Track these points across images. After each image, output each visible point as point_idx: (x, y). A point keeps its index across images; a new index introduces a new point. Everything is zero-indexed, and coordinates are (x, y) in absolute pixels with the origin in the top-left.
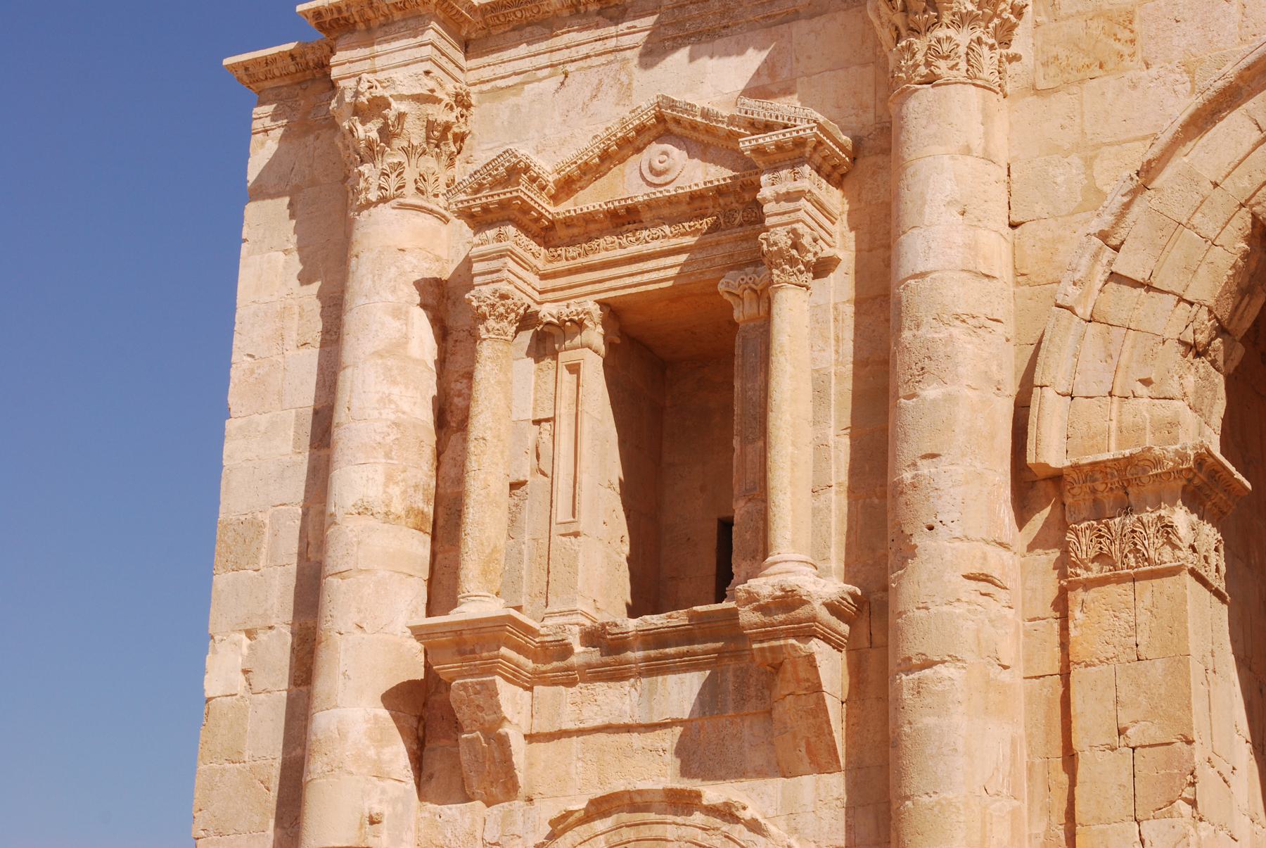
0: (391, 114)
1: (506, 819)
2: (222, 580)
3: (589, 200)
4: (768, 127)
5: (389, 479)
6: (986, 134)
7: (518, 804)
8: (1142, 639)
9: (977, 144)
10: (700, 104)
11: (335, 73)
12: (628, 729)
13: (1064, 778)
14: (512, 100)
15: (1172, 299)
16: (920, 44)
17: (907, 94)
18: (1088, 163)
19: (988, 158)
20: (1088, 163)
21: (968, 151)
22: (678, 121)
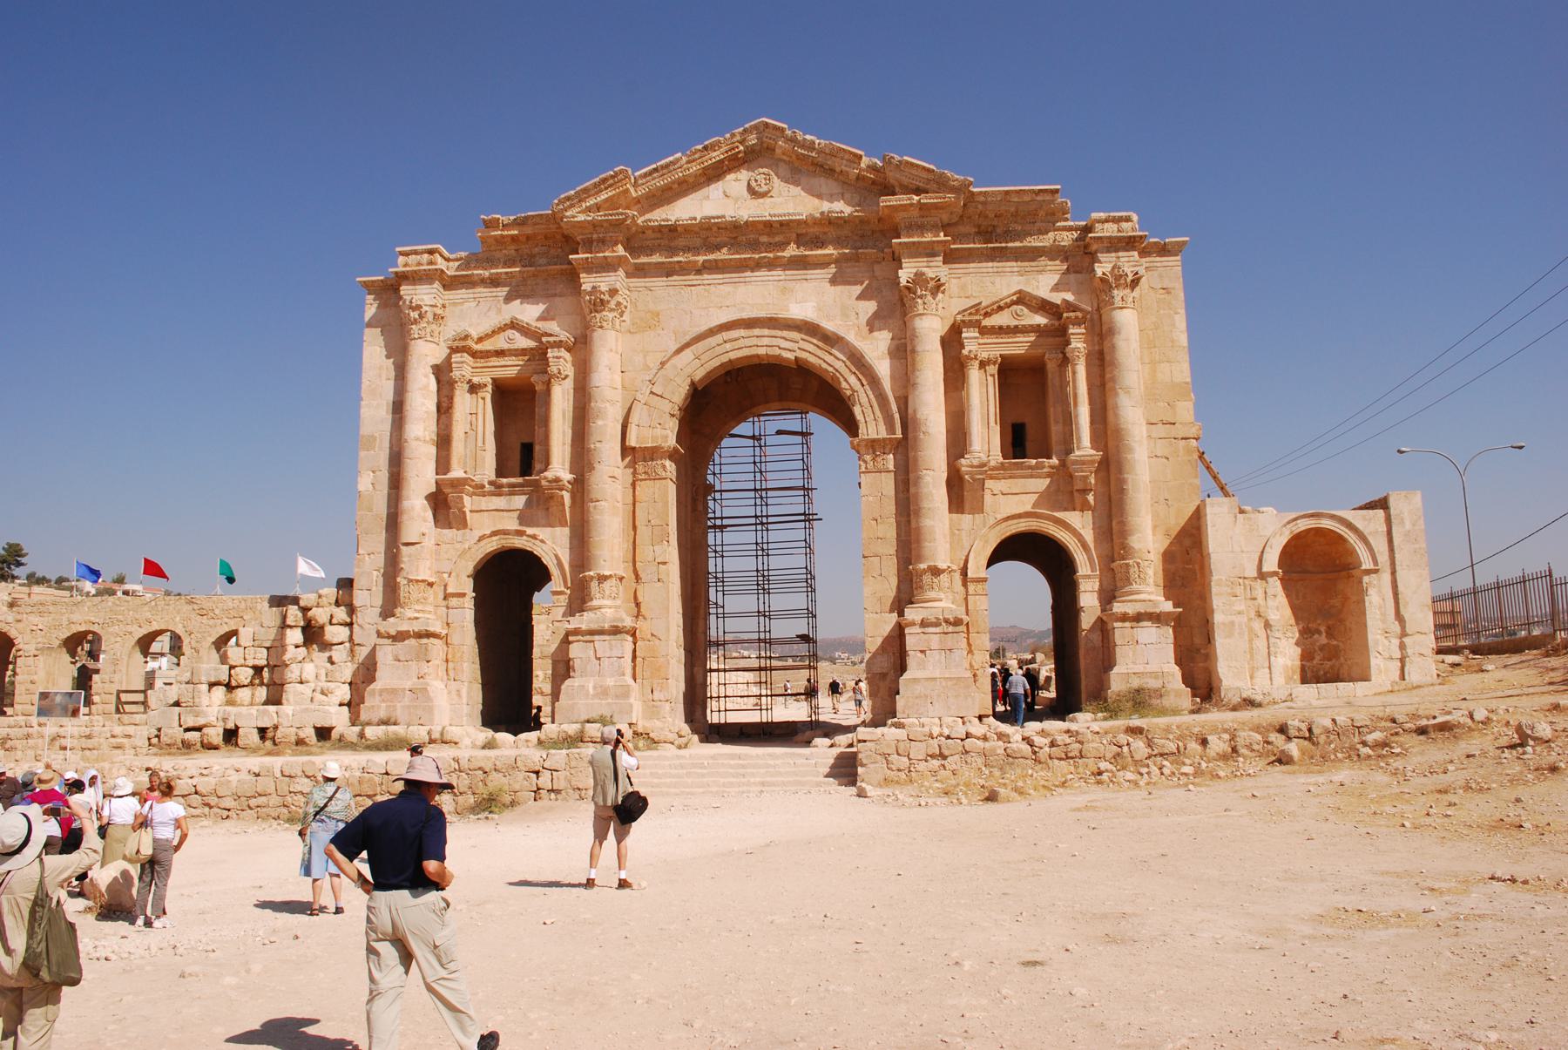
0: (422, 310)
1: (464, 534)
2: (362, 454)
3: (487, 346)
4: (551, 335)
5: (425, 430)
6: (617, 345)
7: (468, 530)
8: (656, 496)
10: (525, 320)
11: (402, 293)
12: (503, 511)
13: (633, 533)
14: (460, 307)
16: (598, 315)
17: (594, 330)
18: (645, 356)
19: (617, 353)
21: (611, 350)
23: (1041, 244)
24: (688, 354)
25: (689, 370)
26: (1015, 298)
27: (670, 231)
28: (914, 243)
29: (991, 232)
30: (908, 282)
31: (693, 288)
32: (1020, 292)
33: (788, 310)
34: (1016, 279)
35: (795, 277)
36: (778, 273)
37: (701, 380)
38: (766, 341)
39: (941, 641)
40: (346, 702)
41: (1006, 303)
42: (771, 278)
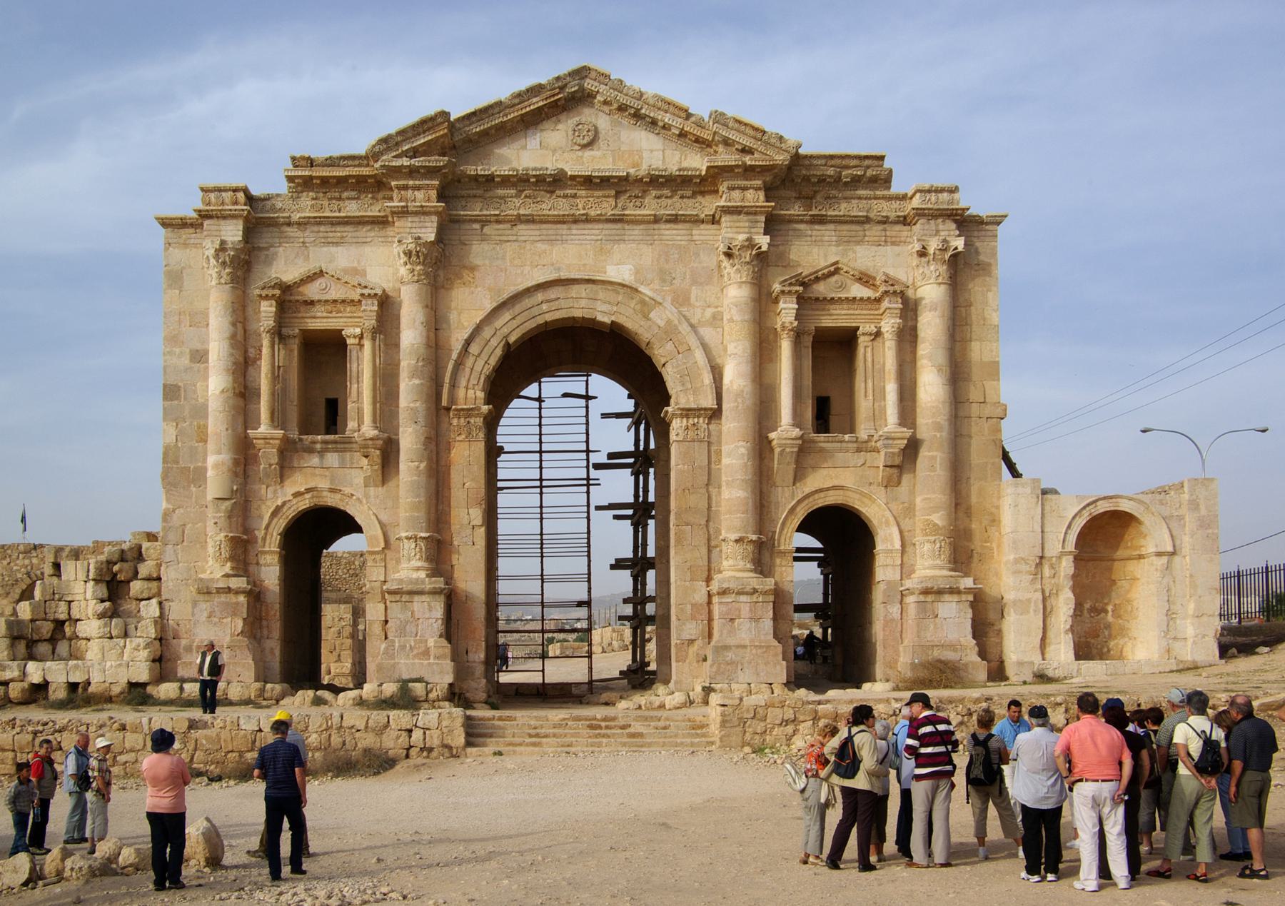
1: (275, 492)
6: (432, 302)
7: (278, 487)
9: (429, 304)
14: (266, 253)
15: (483, 363)
20: (459, 314)
21: (427, 306)
22: (327, 273)
23: (861, 214)
24: (507, 316)
25: (505, 330)
26: (832, 269)
27: (487, 181)
28: (737, 207)
29: (811, 198)
30: (729, 248)
31: (509, 244)
32: (837, 263)
33: (605, 273)
34: (833, 249)
35: (612, 238)
36: (595, 231)
37: (515, 342)
38: (583, 303)
39: (751, 610)
40: (157, 658)
41: (824, 274)
42: (588, 237)
